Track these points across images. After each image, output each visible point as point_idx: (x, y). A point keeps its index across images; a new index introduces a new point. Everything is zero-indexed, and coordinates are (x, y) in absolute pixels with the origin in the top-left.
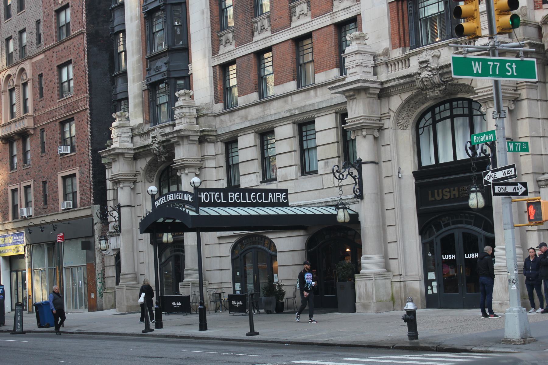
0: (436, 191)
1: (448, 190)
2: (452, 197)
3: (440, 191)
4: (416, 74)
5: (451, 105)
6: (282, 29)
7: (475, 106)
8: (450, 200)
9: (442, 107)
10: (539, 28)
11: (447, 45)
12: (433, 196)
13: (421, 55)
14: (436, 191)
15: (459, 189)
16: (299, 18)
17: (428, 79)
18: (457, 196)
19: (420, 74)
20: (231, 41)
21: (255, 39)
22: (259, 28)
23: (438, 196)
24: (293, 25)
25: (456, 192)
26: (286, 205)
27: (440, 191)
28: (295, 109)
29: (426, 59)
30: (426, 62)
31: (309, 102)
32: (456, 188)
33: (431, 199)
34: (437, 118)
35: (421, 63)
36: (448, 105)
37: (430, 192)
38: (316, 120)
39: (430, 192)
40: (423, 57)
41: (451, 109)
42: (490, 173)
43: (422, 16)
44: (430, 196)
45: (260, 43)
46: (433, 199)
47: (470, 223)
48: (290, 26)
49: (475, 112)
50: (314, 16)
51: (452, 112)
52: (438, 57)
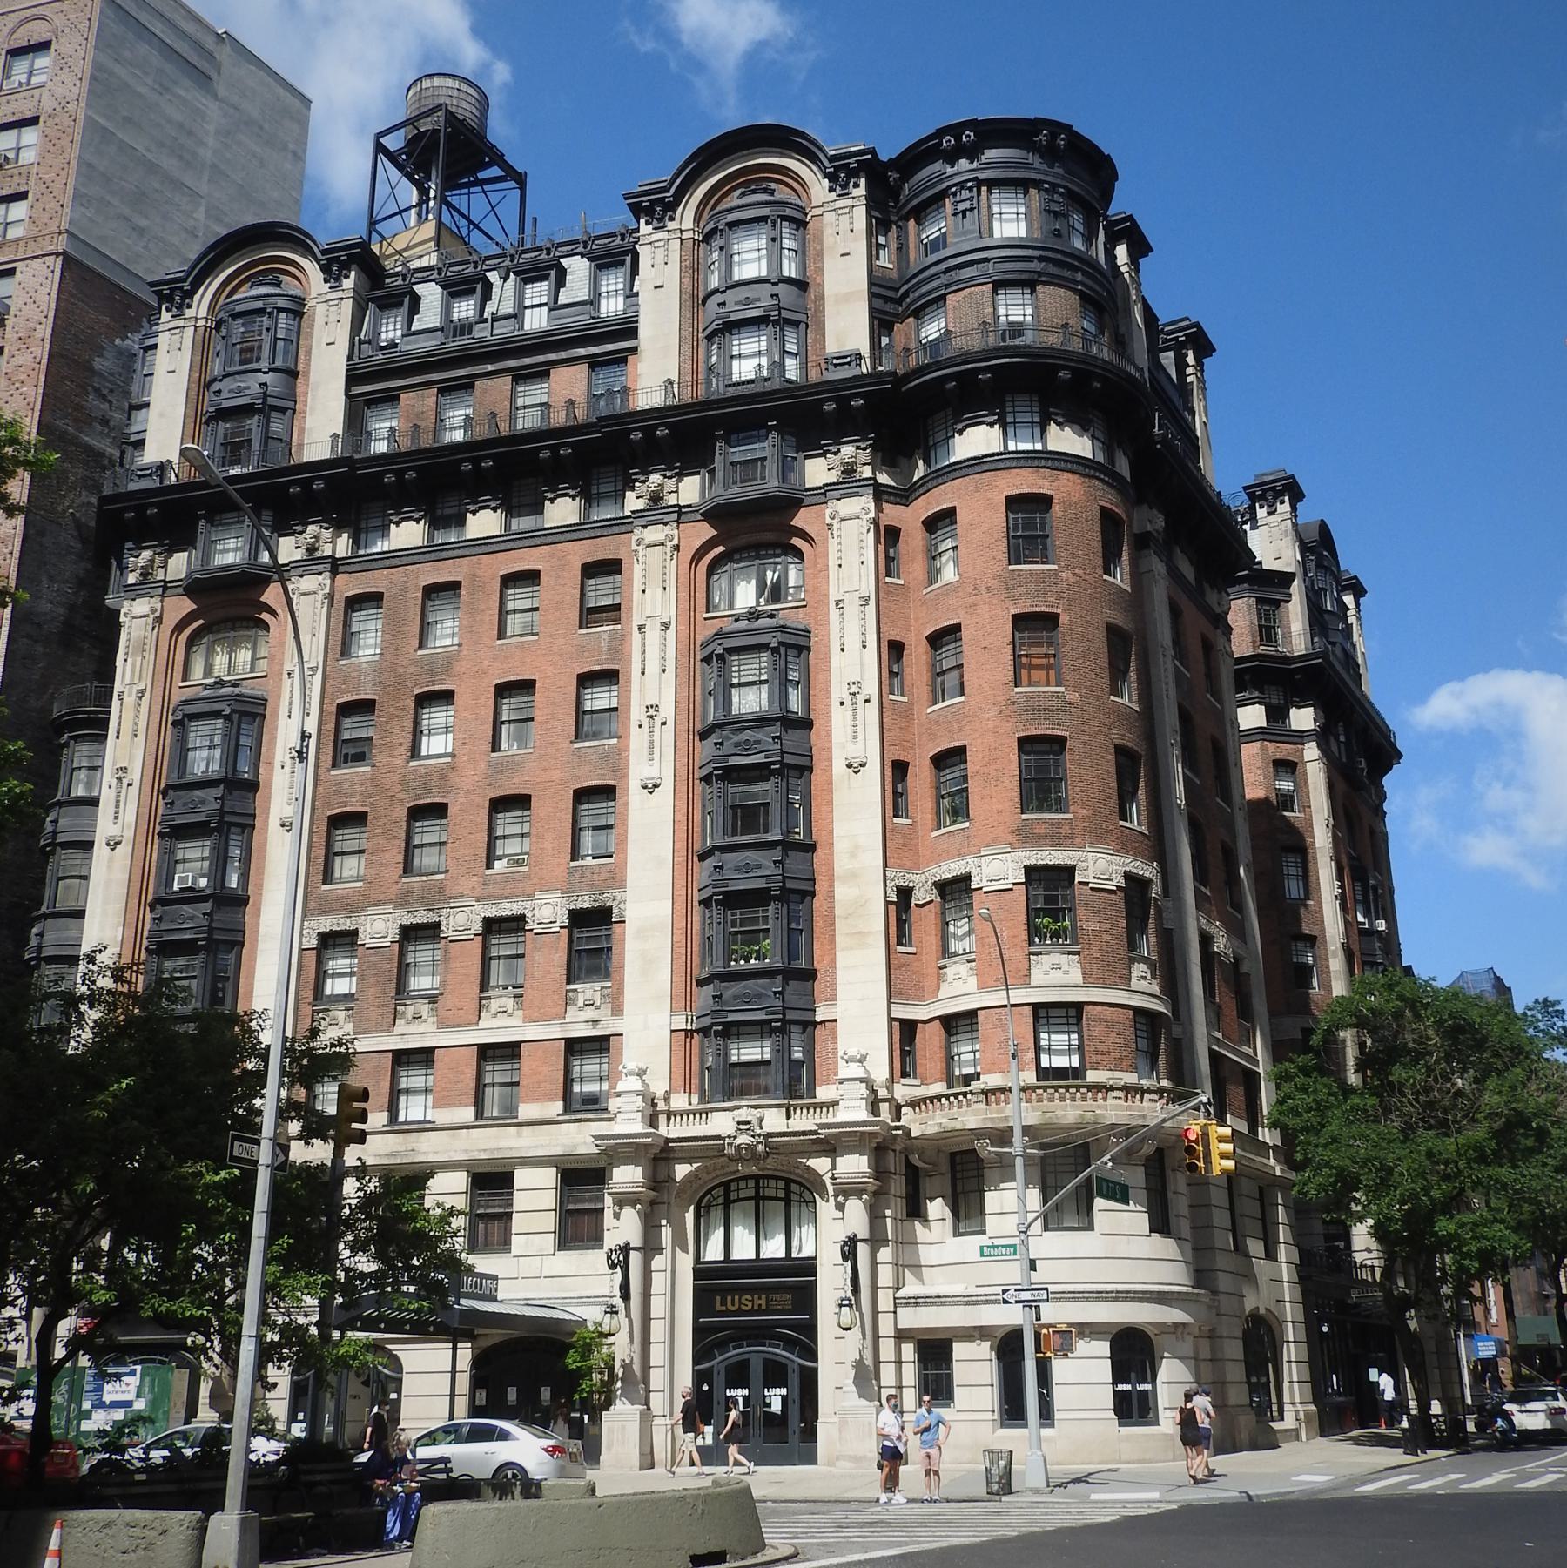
0: (729, 1298)
1: (749, 1297)
2: (756, 1308)
3: (737, 1298)
4: (729, 1137)
5: (757, 1183)
6: (459, 1025)
7: (794, 1187)
8: (751, 1313)
9: (742, 1184)
10: (899, 1107)
11: (779, 1106)
12: (724, 1303)
13: (736, 1112)
14: (729, 1298)
15: (767, 1298)
16: (495, 1016)
17: (751, 1148)
18: (764, 1307)
19: (735, 1137)
20: (341, 1023)
21: (398, 1030)
22: (410, 1016)
23: (733, 1304)
24: (482, 1024)
25: (763, 1302)
26: (494, 1299)
27: (737, 1298)
28: (480, 1151)
29: (749, 1119)
30: (748, 1123)
31: (503, 1144)
32: (764, 1297)
33: (719, 1308)
34: (734, 1196)
35: (739, 1123)
36: (752, 1183)
37: (718, 1298)
38: (517, 1172)
39: (718, 1298)
40: (744, 1114)
41: (757, 1188)
42: (1012, 1292)
43: (734, 1058)
44: (718, 1304)
45: (410, 1038)
46: (724, 1308)
47: (777, 1347)
48: (477, 1024)
49: (794, 1197)
50: (529, 1020)
51: (757, 1192)
52: (761, 1120)
